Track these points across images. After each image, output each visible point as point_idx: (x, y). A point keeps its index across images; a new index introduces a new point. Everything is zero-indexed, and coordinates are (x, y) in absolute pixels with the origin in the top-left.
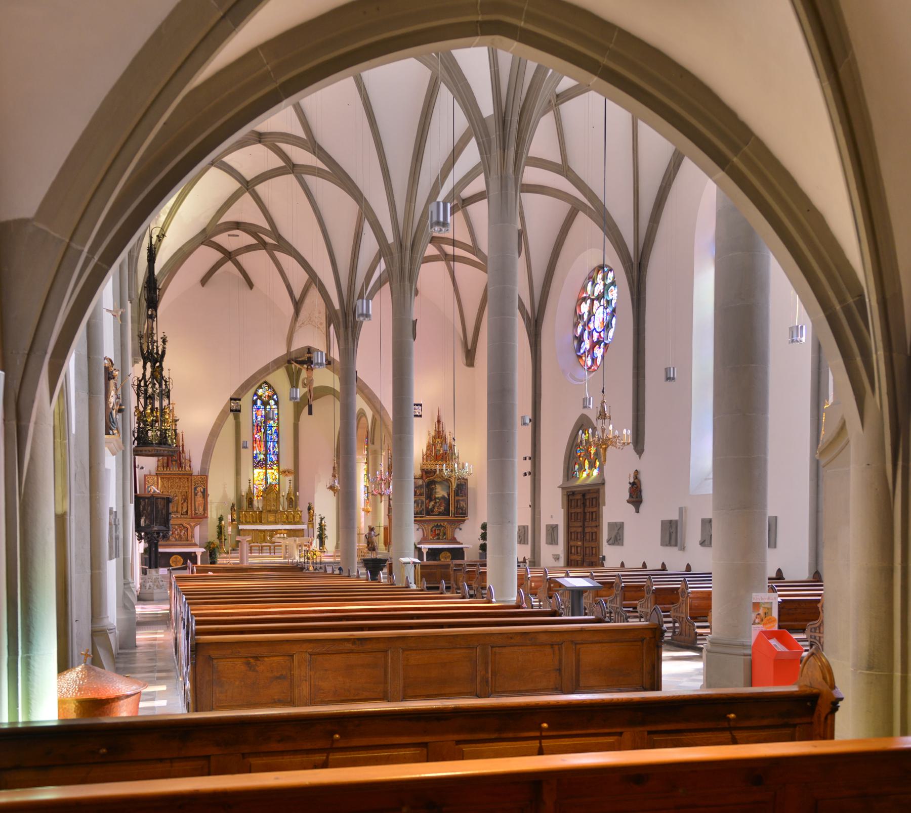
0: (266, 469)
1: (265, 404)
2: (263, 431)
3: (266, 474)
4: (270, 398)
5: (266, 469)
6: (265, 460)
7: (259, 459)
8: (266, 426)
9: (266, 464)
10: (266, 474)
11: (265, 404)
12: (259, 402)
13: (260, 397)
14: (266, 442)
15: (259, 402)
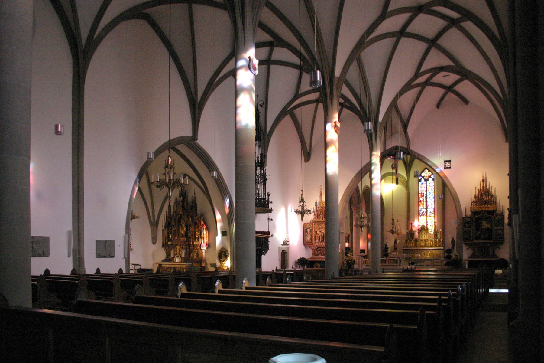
0: (427, 217)
1: (426, 180)
2: (425, 195)
3: (427, 219)
4: (430, 177)
5: (427, 217)
6: (427, 212)
7: (422, 212)
8: (427, 193)
9: (427, 214)
10: (427, 219)
11: (426, 180)
12: (423, 180)
13: (423, 177)
14: (427, 202)
15: (423, 180)
